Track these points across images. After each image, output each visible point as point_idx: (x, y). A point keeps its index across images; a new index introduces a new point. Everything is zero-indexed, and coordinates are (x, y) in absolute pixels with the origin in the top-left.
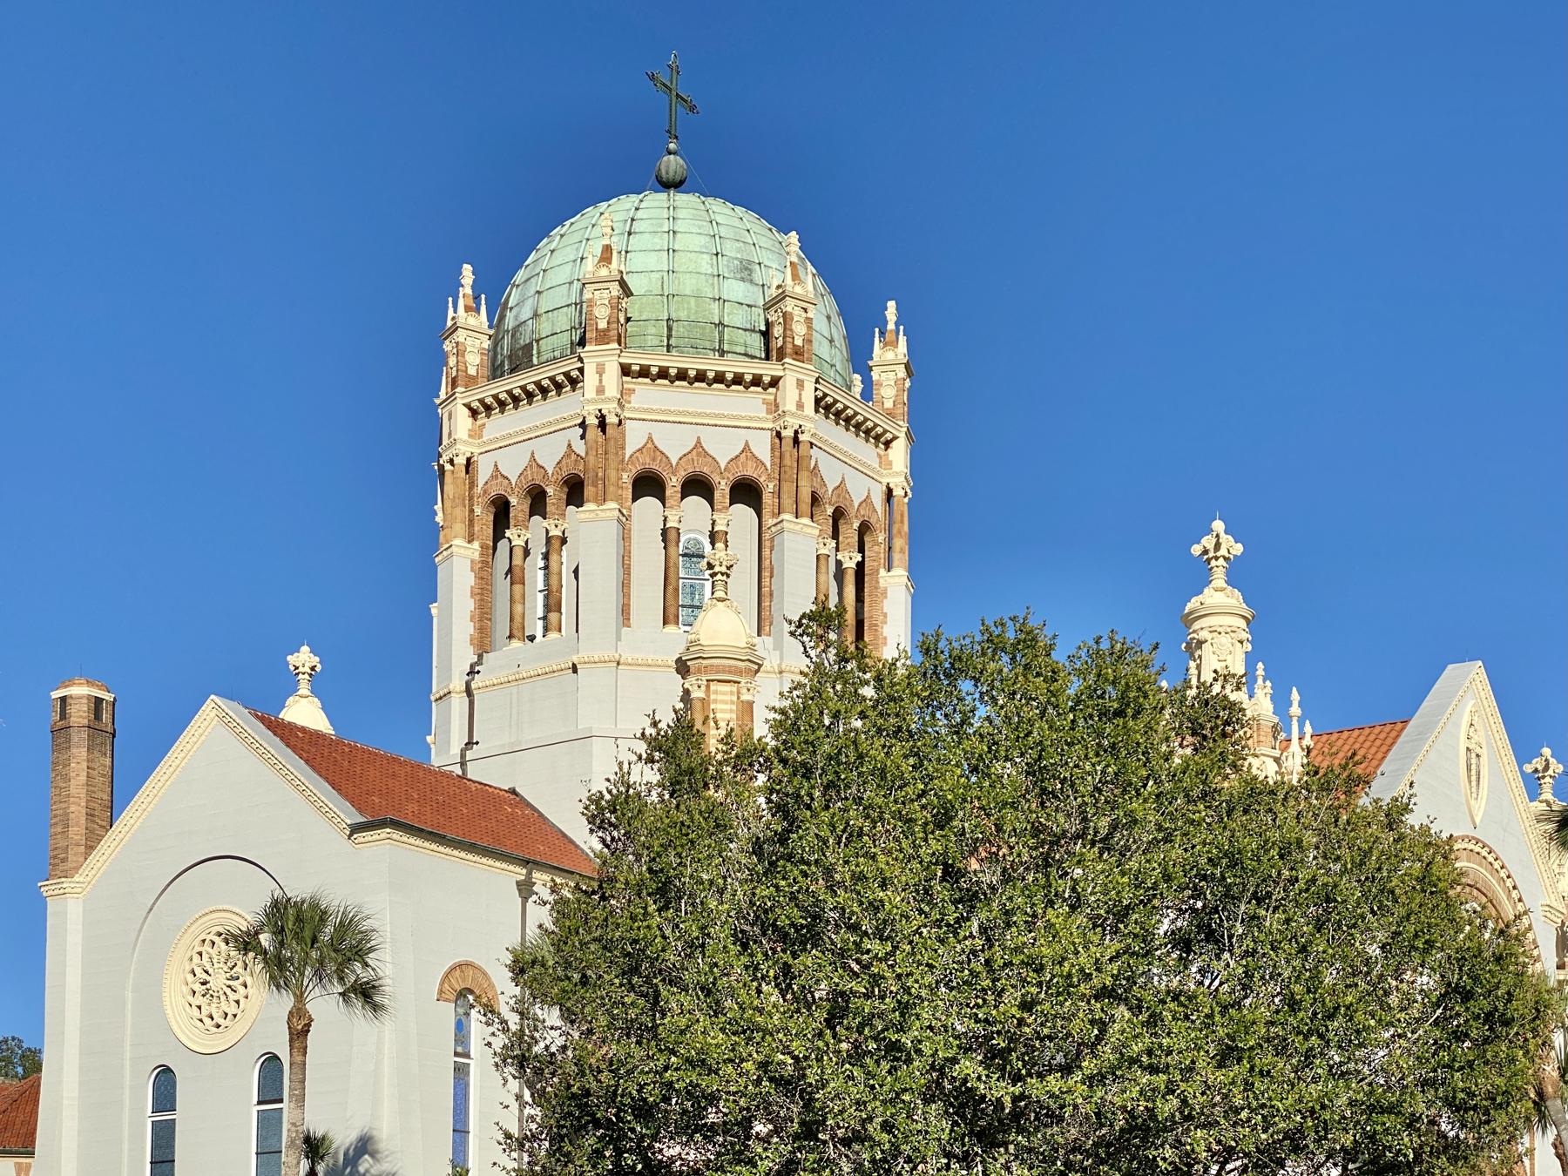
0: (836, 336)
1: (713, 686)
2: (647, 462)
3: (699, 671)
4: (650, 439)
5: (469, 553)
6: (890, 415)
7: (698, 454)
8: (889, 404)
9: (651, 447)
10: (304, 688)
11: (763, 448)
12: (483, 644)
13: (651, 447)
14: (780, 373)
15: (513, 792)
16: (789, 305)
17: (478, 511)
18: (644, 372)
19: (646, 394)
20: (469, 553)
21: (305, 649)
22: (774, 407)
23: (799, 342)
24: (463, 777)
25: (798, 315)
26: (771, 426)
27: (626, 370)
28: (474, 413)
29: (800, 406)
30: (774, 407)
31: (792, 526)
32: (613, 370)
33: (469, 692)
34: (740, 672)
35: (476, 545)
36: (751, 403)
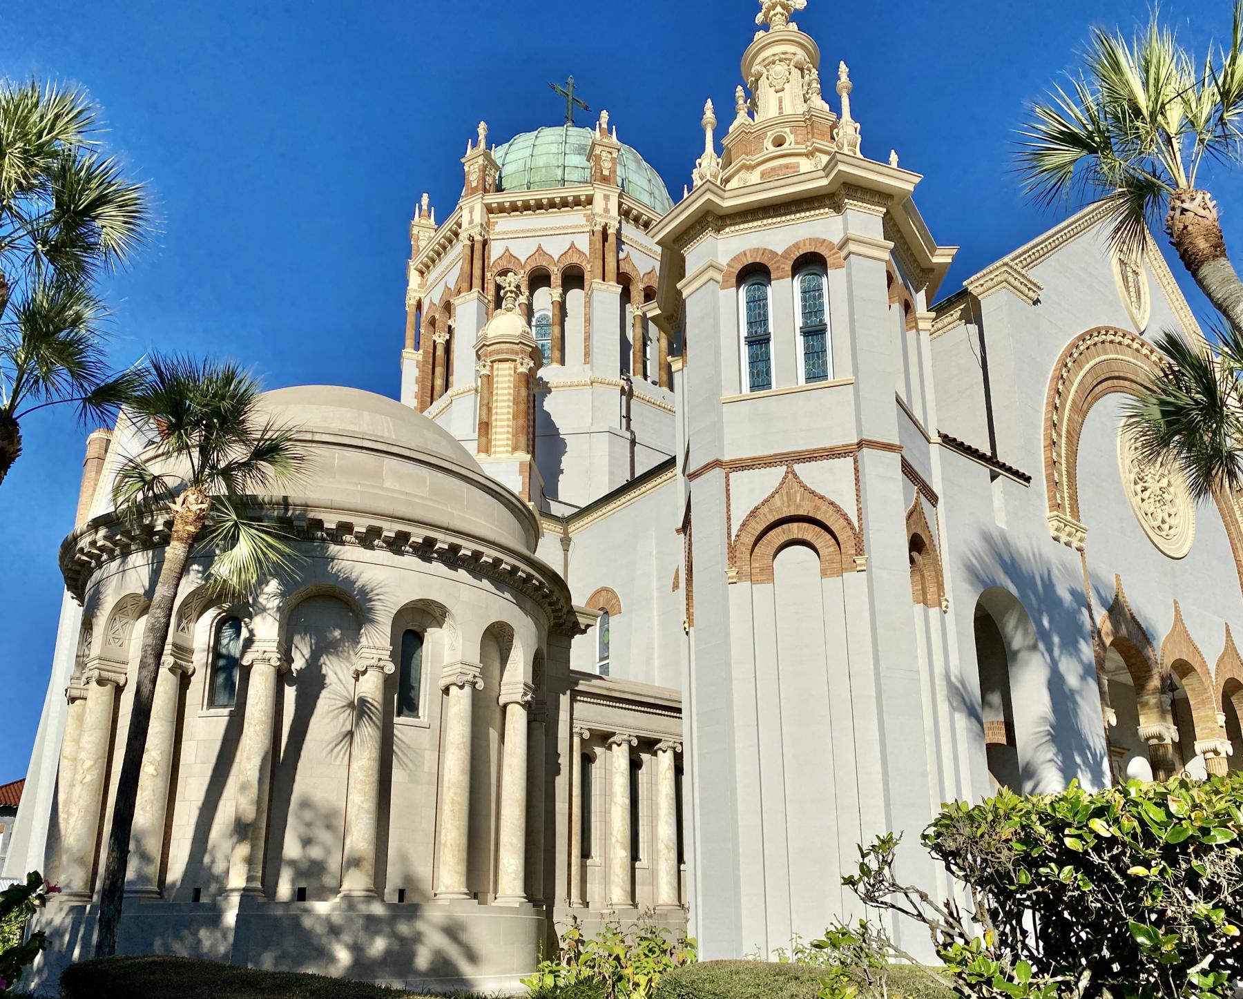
0: (657, 192)
1: (496, 365)
2: (504, 264)
3: (486, 356)
4: (507, 250)
5: (415, 356)
11: (583, 243)
13: (508, 255)
16: (598, 150)
18: (501, 209)
19: (504, 224)
20: (415, 356)
22: (590, 218)
23: (606, 172)
28: (422, 273)
29: (607, 210)
32: (478, 208)
34: (517, 354)
35: (421, 352)
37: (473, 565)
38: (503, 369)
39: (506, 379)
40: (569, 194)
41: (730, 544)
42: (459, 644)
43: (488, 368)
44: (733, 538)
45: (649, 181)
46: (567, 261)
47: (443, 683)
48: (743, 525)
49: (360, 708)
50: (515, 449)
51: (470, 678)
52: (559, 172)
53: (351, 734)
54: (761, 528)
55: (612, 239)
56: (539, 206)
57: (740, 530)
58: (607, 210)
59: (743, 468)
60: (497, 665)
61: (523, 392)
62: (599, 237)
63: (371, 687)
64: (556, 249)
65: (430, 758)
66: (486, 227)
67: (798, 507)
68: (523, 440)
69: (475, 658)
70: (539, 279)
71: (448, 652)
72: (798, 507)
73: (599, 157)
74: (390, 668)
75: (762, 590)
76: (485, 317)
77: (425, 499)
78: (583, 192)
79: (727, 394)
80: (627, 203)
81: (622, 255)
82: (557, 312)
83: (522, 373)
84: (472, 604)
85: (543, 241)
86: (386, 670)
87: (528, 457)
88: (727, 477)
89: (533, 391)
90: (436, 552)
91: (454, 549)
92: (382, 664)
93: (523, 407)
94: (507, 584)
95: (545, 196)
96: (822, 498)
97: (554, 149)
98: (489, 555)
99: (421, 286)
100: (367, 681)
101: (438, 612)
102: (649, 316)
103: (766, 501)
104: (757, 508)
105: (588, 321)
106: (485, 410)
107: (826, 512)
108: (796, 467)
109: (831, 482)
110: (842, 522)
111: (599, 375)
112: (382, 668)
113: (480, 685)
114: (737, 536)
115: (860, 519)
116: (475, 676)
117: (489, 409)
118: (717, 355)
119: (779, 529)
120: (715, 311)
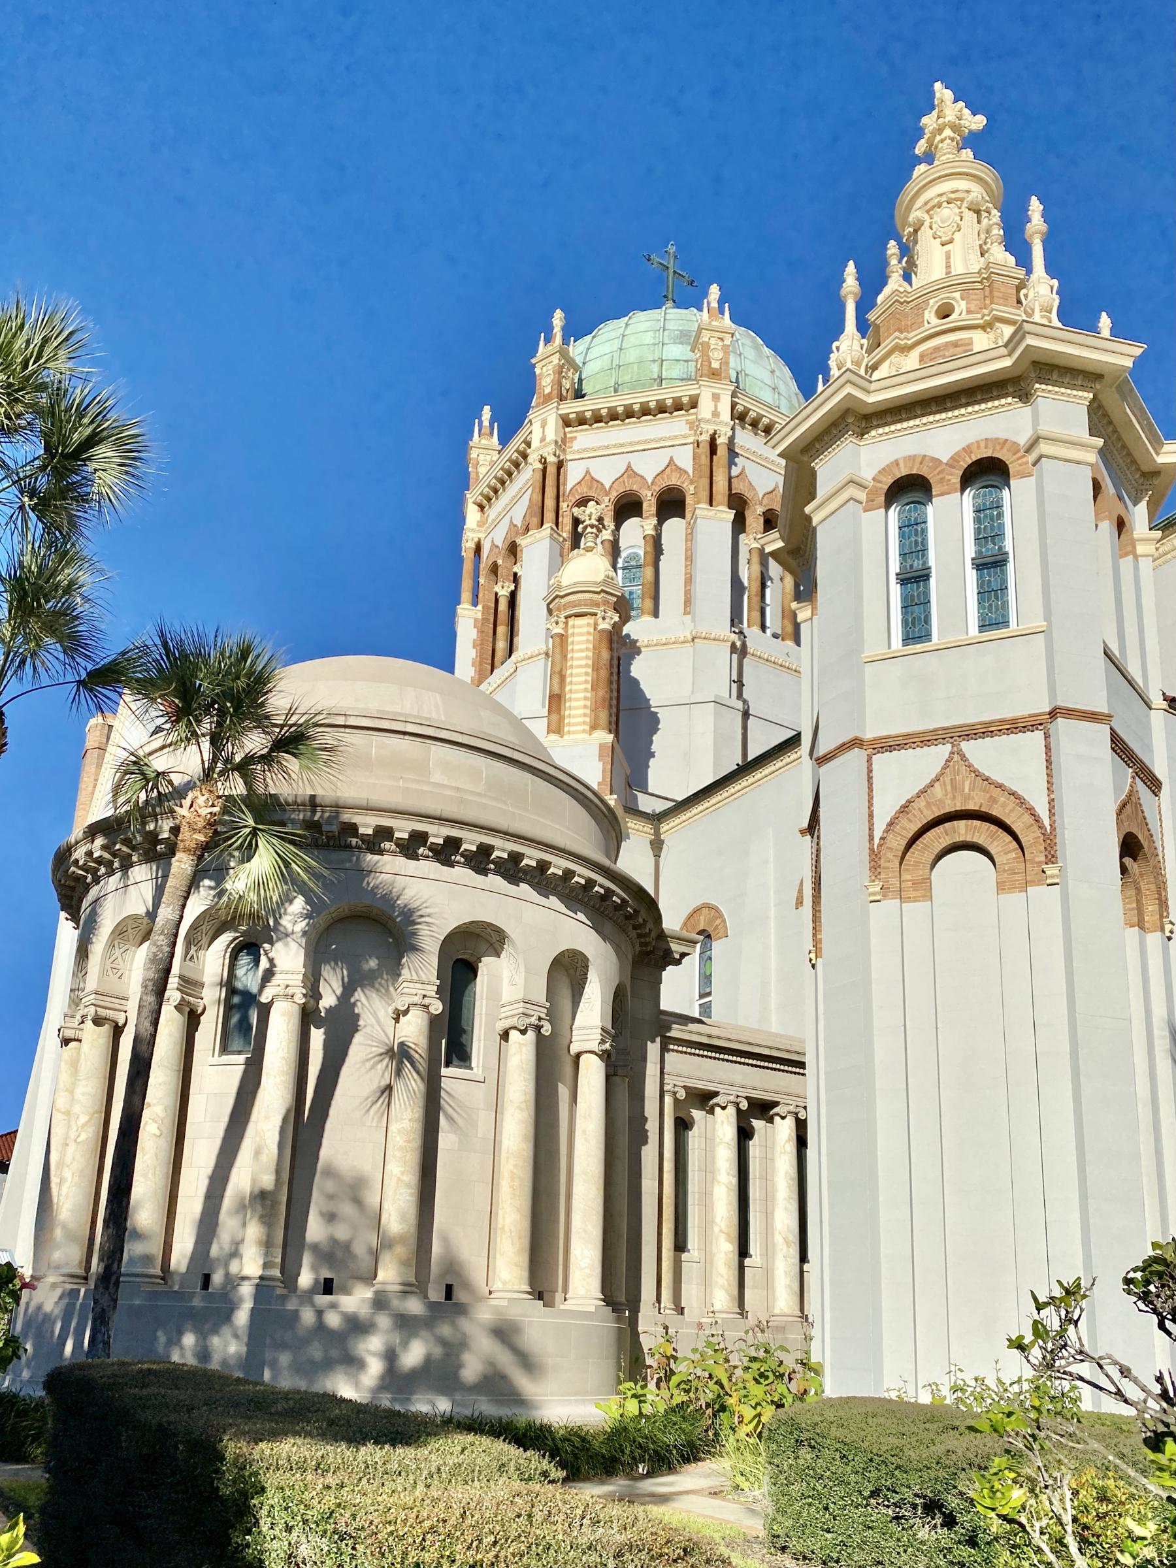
0: (782, 388)
1: (571, 622)
3: (559, 610)
7: (629, 477)
9: (589, 479)
11: (685, 459)
13: (589, 479)
14: (697, 392)
22: (694, 426)
23: (716, 365)
26: (691, 440)
29: (716, 414)
31: (705, 513)
34: (597, 605)
37: (539, 878)
38: (581, 627)
39: (583, 639)
40: (667, 395)
41: (871, 849)
42: (520, 979)
43: (561, 625)
44: (877, 841)
45: (773, 372)
46: (664, 483)
47: (501, 1026)
48: (891, 824)
49: (400, 1055)
50: (594, 727)
51: (534, 1020)
52: (655, 368)
53: (389, 1088)
54: (915, 827)
55: (722, 451)
56: (629, 414)
57: (887, 831)
58: (716, 414)
59: (891, 748)
60: (567, 1004)
61: (605, 654)
62: (705, 449)
63: (413, 1031)
64: (649, 468)
65: (484, 1119)
67: (968, 798)
68: (604, 716)
69: (541, 996)
70: (627, 507)
71: (506, 987)
72: (968, 798)
73: (707, 346)
74: (437, 1007)
75: (915, 911)
76: (559, 560)
77: (480, 795)
78: (684, 392)
79: (868, 653)
80: (743, 403)
81: (735, 471)
82: (650, 549)
83: (603, 630)
84: (539, 928)
86: (432, 1010)
87: (610, 738)
88: (869, 760)
89: (619, 651)
90: (493, 862)
91: (516, 858)
92: (427, 1001)
93: (604, 673)
94: (581, 902)
95: (635, 400)
96: (1000, 786)
97: (648, 338)
98: (558, 866)
100: (409, 1023)
101: (495, 937)
102: (768, 549)
103: (923, 791)
104: (909, 802)
105: (690, 558)
106: (556, 680)
107: (1004, 806)
108: (965, 746)
109: (1013, 764)
110: (1028, 819)
111: (703, 629)
112: (427, 1007)
113: (547, 1029)
114: (882, 838)
115: (1052, 814)
116: (540, 1019)
117: (562, 678)
118: (859, 598)
119: (939, 829)
120: (858, 540)
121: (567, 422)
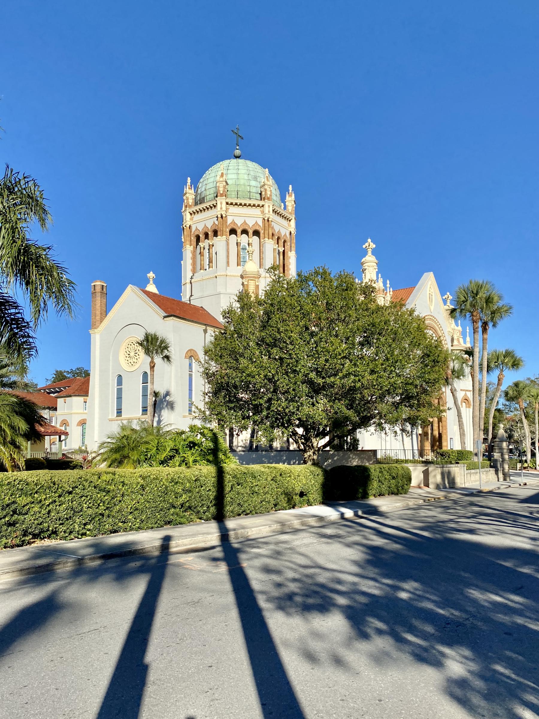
1: (249, 281)
2: (233, 226)
6: (291, 213)
8: (290, 211)
9: (233, 222)
10: (151, 282)
11: (260, 222)
12: (194, 271)
13: (233, 222)
15: (202, 307)
16: (266, 187)
17: (192, 238)
18: (232, 204)
19: (233, 210)
21: (151, 272)
22: (263, 212)
23: (268, 196)
24: (190, 304)
25: (268, 189)
27: (227, 203)
28: (191, 214)
29: (269, 212)
30: (263, 212)
33: (191, 283)
34: (255, 278)
35: (192, 247)
36: (257, 211)
46: (254, 228)
66: (227, 209)
85: (246, 218)
99: (192, 219)
121: (227, 203)
